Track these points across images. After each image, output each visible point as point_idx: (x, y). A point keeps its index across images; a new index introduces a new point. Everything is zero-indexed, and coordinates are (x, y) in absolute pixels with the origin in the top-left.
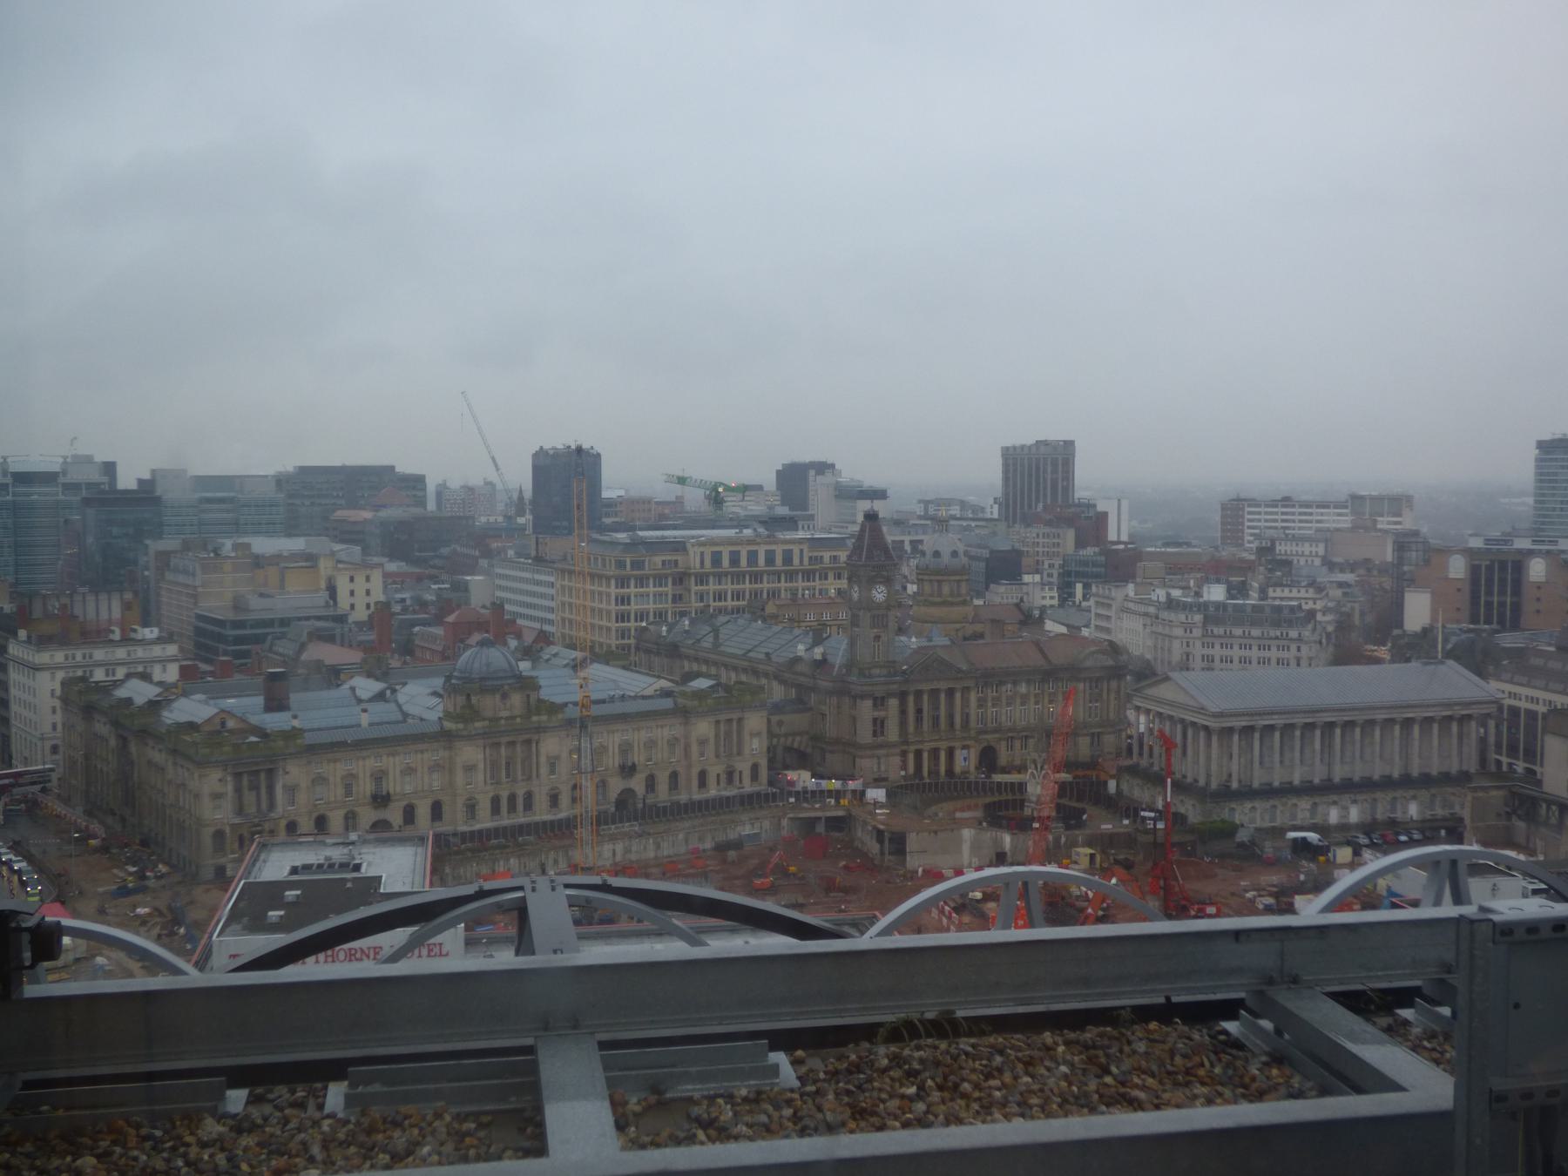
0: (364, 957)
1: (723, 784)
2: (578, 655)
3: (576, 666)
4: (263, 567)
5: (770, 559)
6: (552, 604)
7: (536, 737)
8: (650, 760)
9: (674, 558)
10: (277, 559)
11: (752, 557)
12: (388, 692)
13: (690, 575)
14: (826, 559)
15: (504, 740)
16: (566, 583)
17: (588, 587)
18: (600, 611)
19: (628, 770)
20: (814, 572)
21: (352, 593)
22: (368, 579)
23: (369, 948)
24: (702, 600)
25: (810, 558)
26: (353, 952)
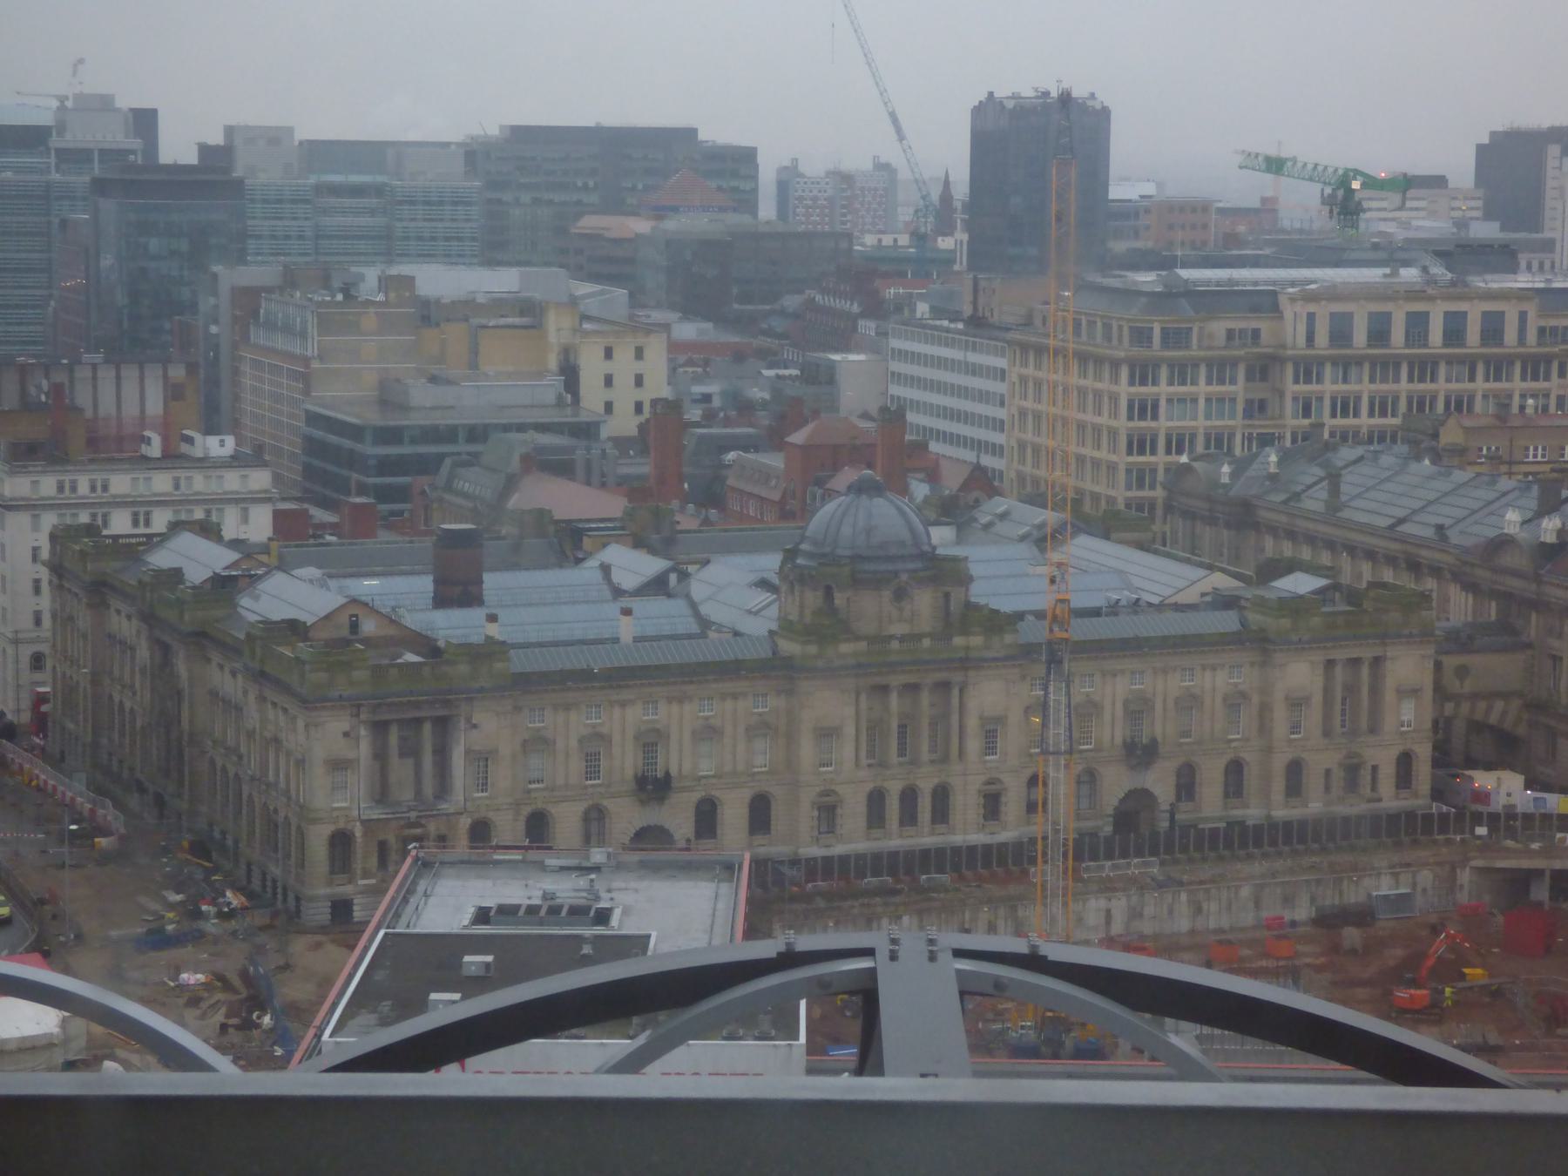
2: (1049, 517)
3: (1043, 540)
4: (438, 325)
5: (1454, 333)
6: (1001, 413)
7: (957, 677)
8: (1186, 734)
9: (1254, 325)
10: (464, 309)
11: (1417, 324)
12: (673, 578)
13: (1282, 361)
15: (896, 680)
16: (1030, 371)
17: (1075, 380)
18: (1097, 429)
19: (1141, 753)
20: (1548, 359)
21: (609, 381)
22: (639, 354)
24: (1307, 412)
25: (1542, 331)
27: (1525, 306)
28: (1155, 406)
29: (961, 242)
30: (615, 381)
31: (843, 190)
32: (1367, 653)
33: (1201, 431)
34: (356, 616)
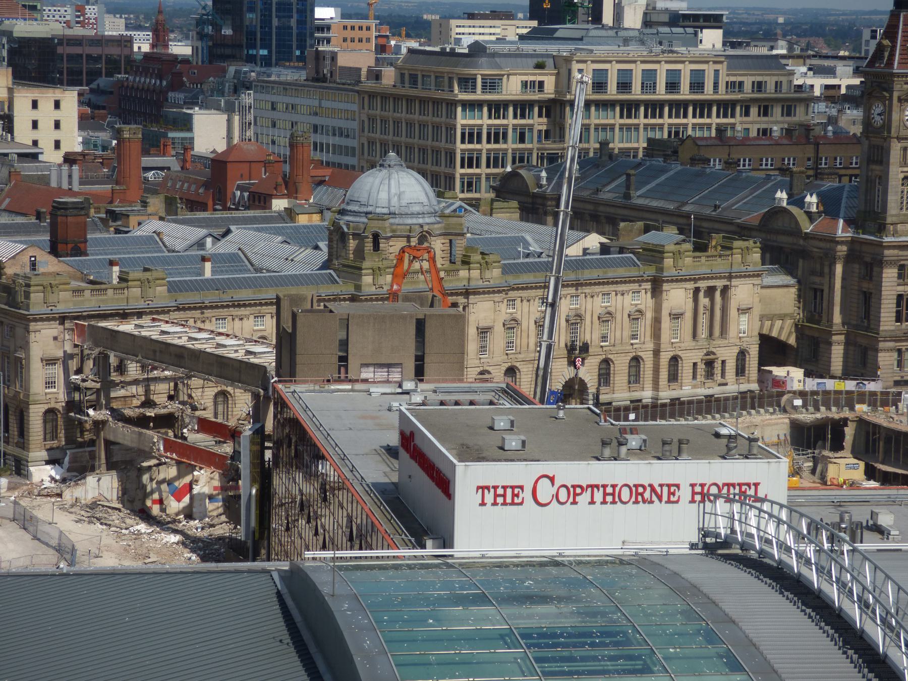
0: (654, 498)
1: (700, 378)
5: (672, 86)
12: (209, 240)
14: (748, 87)
20: (733, 104)
21: (35, 125)
22: (57, 105)
23: (661, 486)
26: (641, 490)
27: (718, 67)
28: (479, 135)
29: (197, 48)
30: (40, 125)
31: (78, 17)
32: (720, 283)
33: (510, 151)
34: (35, 257)
